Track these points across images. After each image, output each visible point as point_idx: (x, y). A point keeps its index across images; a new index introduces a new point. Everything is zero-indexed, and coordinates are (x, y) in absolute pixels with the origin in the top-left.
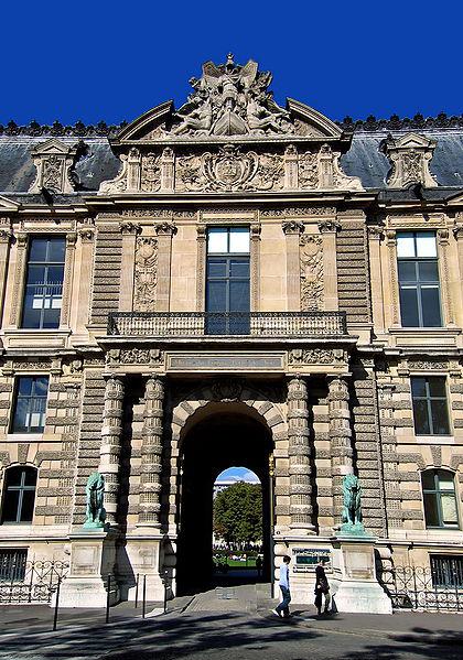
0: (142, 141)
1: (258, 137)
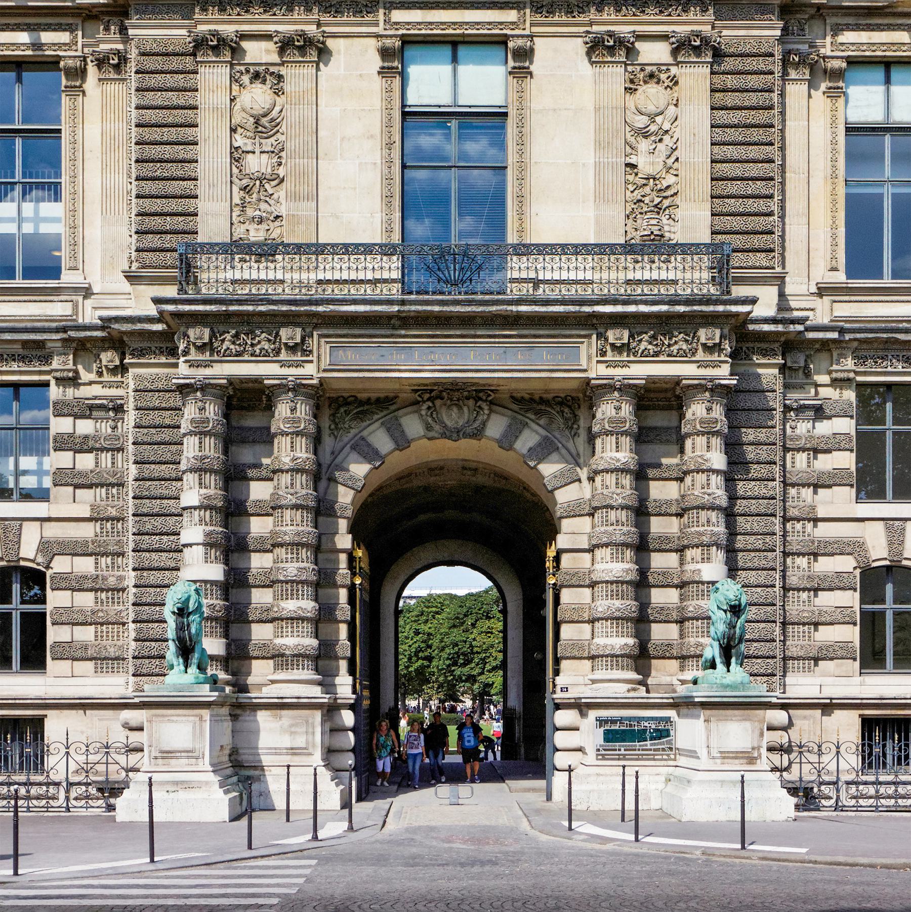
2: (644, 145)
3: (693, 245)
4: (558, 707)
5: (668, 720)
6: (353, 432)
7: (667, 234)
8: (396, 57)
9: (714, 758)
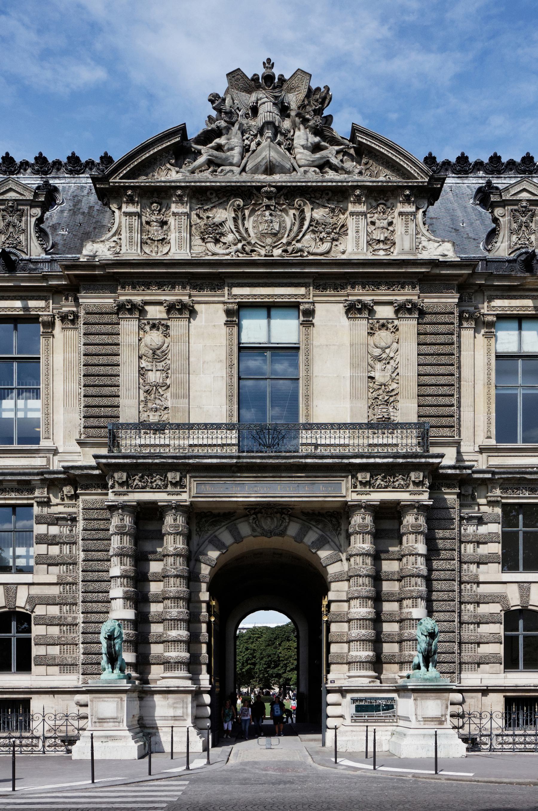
0: (142, 180)
1: (313, 177)
2: (379, 366)
3: (407, 423)
4: (329, 692)
5: (392, 699)
6: (210, 532)
7: (392, 417)
8: (234, 315)
9: (419, 721)
